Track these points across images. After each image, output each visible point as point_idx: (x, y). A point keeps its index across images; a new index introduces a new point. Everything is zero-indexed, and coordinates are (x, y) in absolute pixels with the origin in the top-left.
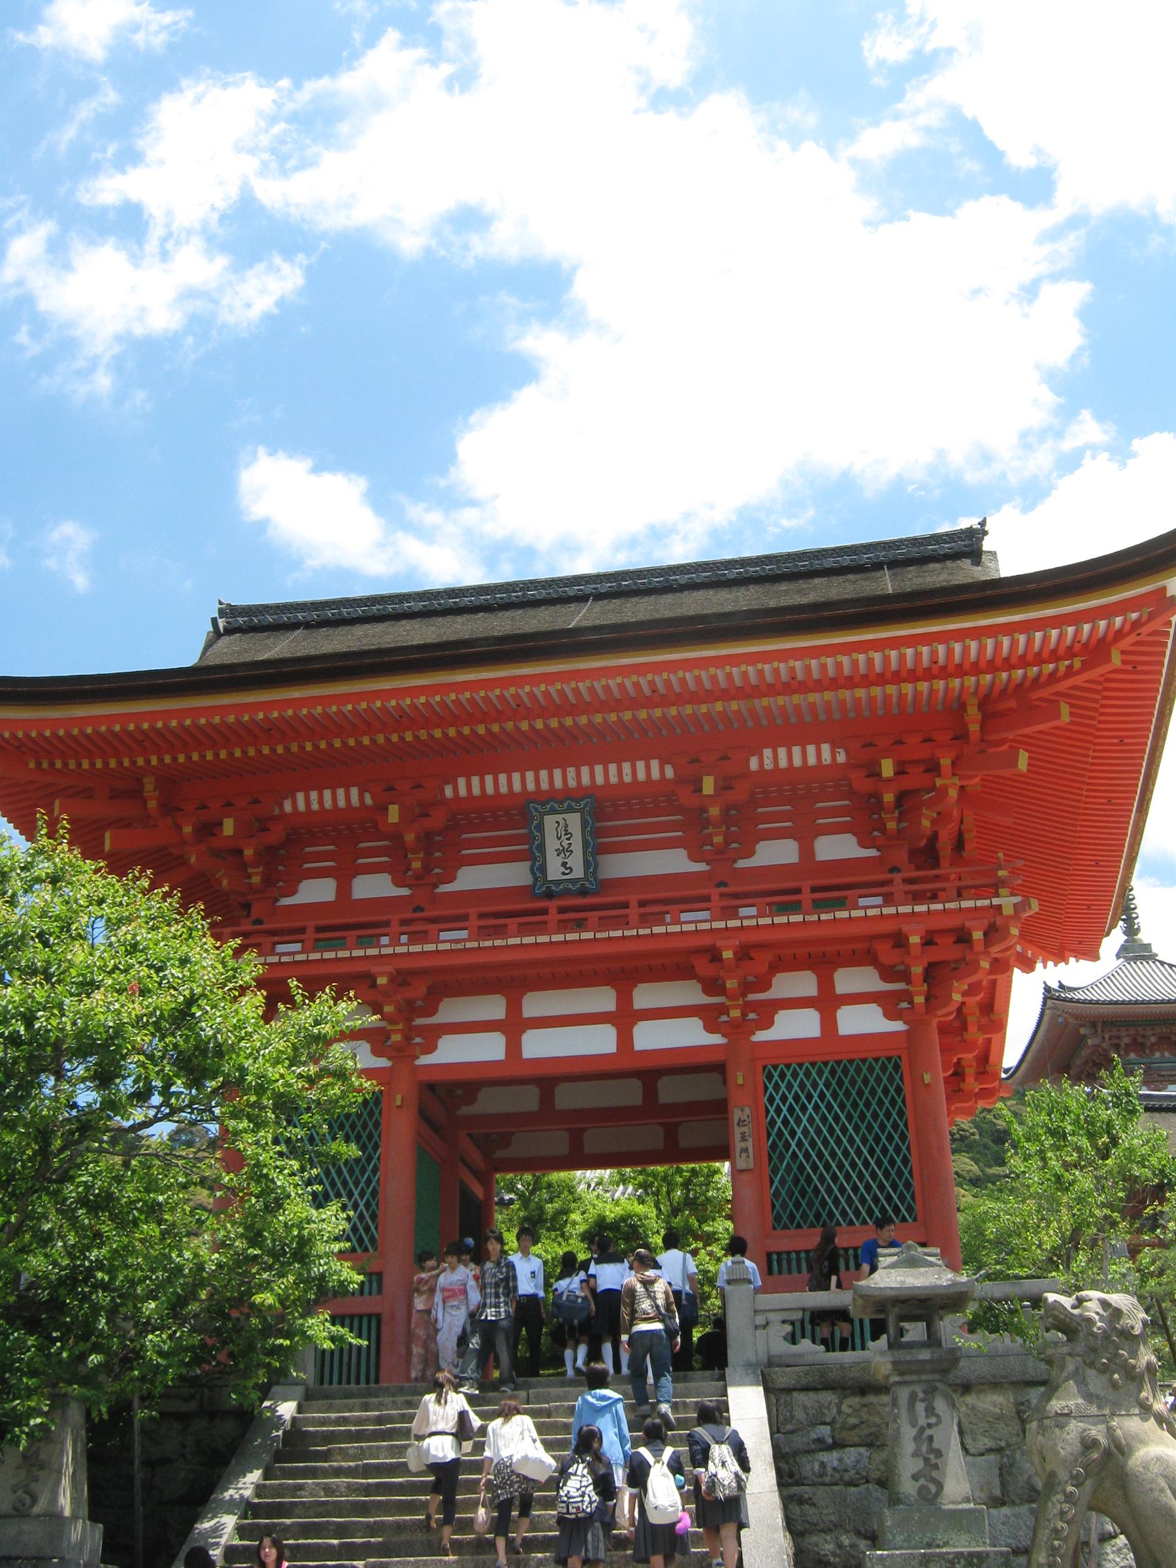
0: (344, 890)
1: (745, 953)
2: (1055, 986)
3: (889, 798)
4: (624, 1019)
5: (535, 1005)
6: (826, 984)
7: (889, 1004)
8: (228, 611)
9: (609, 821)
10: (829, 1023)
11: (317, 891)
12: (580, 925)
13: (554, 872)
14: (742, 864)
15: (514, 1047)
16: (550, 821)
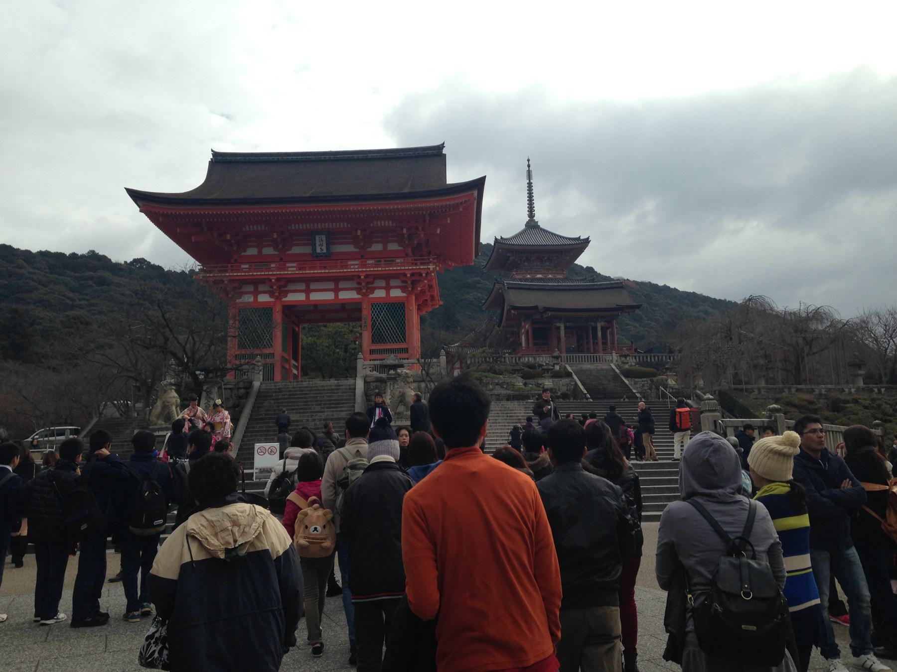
0: (260, 251)
1: (367, 276)
2: (499, 238)
3: (406, 236)
4: (336, 290)
5: (313, 286)
6: (388, 284)
7: (403, 289)
8: (215, 154)
9: (332, 237)
10: (388, 293)
11: (252, 251)
12: (325, 268)
13: (318, 250)
14: (369, 249)
15: (308, 297)
16: (317, 237)
